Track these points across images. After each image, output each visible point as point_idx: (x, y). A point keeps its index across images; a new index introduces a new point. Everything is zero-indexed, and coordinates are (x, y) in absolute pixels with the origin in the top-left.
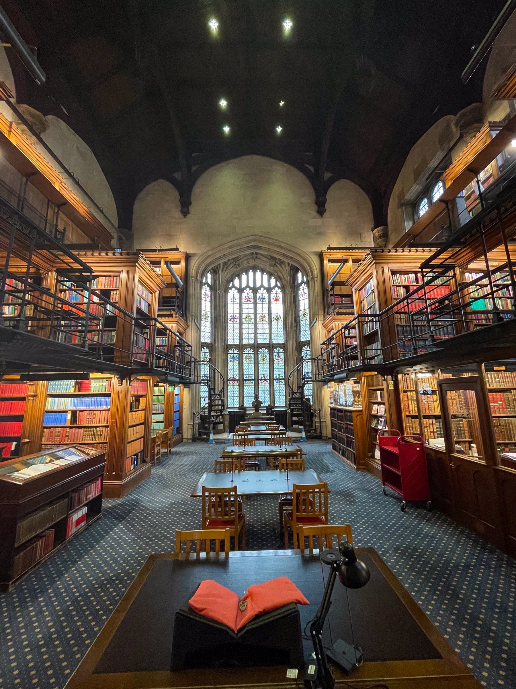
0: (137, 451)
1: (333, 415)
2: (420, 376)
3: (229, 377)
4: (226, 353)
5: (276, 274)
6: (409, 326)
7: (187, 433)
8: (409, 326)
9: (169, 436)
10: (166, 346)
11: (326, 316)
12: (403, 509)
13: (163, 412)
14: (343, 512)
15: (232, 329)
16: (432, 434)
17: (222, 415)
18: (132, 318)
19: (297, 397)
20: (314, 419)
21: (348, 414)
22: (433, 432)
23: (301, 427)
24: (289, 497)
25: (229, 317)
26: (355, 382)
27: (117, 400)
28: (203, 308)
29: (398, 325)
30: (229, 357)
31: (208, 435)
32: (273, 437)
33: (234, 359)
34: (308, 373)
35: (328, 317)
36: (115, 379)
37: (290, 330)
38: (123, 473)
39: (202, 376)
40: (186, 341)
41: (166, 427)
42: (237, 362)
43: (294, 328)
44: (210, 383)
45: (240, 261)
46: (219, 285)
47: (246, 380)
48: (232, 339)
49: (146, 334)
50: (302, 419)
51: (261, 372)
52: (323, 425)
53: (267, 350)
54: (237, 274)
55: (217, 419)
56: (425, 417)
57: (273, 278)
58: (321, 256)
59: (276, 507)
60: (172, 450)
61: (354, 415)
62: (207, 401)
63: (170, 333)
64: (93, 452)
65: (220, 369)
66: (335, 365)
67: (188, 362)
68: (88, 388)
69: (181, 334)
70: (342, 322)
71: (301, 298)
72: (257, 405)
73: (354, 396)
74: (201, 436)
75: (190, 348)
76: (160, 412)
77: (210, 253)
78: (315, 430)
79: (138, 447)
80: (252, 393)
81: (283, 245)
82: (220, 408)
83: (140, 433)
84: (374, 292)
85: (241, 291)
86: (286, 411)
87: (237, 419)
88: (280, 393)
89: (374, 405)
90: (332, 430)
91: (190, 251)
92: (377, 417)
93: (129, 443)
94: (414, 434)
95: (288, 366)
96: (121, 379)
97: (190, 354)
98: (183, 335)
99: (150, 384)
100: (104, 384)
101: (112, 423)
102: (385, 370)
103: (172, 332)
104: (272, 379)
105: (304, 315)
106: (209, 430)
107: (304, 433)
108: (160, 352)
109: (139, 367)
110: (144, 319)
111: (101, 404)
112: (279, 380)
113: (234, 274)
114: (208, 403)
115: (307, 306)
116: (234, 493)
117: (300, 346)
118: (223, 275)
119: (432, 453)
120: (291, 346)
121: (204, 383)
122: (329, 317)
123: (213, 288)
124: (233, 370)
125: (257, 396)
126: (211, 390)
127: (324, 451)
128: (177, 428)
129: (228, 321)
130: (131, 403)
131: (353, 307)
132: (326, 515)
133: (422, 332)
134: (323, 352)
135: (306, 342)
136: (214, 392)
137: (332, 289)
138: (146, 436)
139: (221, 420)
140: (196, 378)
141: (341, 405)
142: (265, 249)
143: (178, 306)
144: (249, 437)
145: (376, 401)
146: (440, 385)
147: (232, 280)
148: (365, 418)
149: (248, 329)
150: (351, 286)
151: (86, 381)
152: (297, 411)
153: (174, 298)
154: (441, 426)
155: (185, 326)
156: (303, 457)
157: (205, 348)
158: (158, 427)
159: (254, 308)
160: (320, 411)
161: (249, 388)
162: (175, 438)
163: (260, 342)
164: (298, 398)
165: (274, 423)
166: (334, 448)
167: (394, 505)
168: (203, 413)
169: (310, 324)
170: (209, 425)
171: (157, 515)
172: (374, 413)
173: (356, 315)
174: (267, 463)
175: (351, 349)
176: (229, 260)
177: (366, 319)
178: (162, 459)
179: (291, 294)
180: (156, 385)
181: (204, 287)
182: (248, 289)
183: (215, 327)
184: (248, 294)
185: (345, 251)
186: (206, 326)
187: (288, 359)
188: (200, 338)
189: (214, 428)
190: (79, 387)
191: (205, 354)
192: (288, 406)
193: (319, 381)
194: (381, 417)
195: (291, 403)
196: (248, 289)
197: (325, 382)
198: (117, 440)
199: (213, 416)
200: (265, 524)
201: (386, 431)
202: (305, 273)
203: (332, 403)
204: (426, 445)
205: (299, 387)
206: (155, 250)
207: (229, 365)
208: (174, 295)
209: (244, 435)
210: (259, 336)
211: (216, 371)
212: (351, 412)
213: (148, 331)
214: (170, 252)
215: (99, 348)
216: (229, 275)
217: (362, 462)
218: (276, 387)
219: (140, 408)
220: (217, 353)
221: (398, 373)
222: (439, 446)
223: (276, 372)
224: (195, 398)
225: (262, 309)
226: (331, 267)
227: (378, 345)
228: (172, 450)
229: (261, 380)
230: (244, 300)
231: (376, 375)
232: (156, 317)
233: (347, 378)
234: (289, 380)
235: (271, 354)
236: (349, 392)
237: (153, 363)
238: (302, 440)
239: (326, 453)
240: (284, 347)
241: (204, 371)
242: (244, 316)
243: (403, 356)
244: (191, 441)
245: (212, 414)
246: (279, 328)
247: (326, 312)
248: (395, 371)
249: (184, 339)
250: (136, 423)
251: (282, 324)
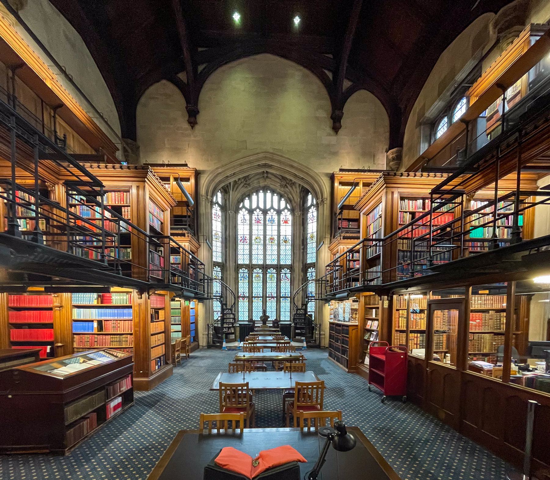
0: (160, 355)
1: (331, 328)
2: (412, 297)
4: (237, 272)
6: (410, 251)
7: (203, 341)
8: (410, 251)
9: (187, 343)
10: (179, 264)
11: (332, 240)
12: (383, 401)
13: (180, 323)
14: (334, 403)
15: (243, 250)
16: (415, 346)
17: (233, 327)
18: (146, 235)
20: (314, 331)
21: (345, 328)
22: (417, 344)
23: (303, 338)
24: (291, 392)
25: (239, 238)
26: (354, 301)
27: (138, 311)
28: (214, 228)
29: (399, 250)
30: (239, 276)
31: (221, 343)
32: (278, 345)
33: (244, 278)
34: (311, 293)
36: (135, 293)
37: (297, 252)
38: (150, 372)
41: (184, 336)
42: (247, 281)
48: (243, 259)
49: (160, 252)
50: (304, 331)
53: (275, 270)
56: (412, 332)
60: (190, 354)
61: (350, 329)
62: (220, 315)
64: (121, 355)
65: (232, 287)
66: (337, 286)
67: (201, 280)
68: (110, 300)
70: (348, 246)
71: (309, 221)
72: (265, 318)
75: (203, 266)
76: (177, 323)
78: (315, 341)
79: (160, 352)
80: (261, 309)
82: (231, 320)
83: (161, 340)
85: (251, 212)
86: (291, 324)
87: (247, 330)
88: (285, 309)
90: (330, 341)
92: (370, 331)
93: (152, 348)
94: (400, 345)
95: (293, 285)
96: (141, 292)
98: (196, 254)
99: (167, 298)
100: (125, 297)
101: (135, 331)
102: (382, 291)
105: (312, 237)
107: (305, 343)
109: (156, 283)
110: (157, 236)
111: (124, 315)
115: (315, 230)
116: (245, 388)
117: (306, 267)
119: (413, 360)
120: (298, 267)
122: (335, 241)
124: (243, 288)
125: (264, 312)
126: (224, 305)
127: (322, 357)
129: (239, 242)
130: (152, 315)
131: (359, 232)
132: (321, 405)
133: (420, 257)
134: (327, 273)
135: (311, 264)
136: (226, 307)
138: (167, 342)
139: (233, 331)
140: (209, 294)
141: (339, 321)
143: (189, 225)
144: (258, 345)
145: (371, 317)
146: (429, 305)
148: (359, 331)
149: (258, 250)
151: (107, 295)
153: (185, 217)
154: (424, 339)
155: (197, 245)
156: (304, 361)
158: (176, 336)
161: (257, 304)
162: (193, 345)
163: (268, 262)
165: (279, 335)
166: (330, 355)
167: (376, 398)
168: (216, 325)
169: (317, 247)
170: (222, 335)
171: (181, 404)
172: (368, 327)
173: (361, 239)
174: (273, 366)
175: (353, 272)
178: (181, 362)
179: (300, 216)
180: (173, 300)
182: (258, 210)
183: (226, 247)
186: (217, 246)
187: (294, 279)
188: (212, 258)
189: (226, 338)
190: (102, 299)
191: (217, 273)
192: (292, 320)
193: (321, 300)
194: (373, 331)
196: (258, 210)
197: (327, 301)
198: (141, 345)
199: (225, 327)
200: (270, 411)
201: (377, 343)
204: (409, 354)
205: (303, 305)
209: (254, 343)
210: (268, 257)
212: (347, 326)
213: (162, 249)
215: (117, 265)
217: (353, 367)
218: (282, 304)
219: (160, 319)
220: (228, 272)
221: (393, 294)
222: (420, 355)
223: (283, 290)
224: (209, 312)
227: (379, 268)
228: (190, 354)
229: (269, 297)
230: (253, 222)
232: (169, 235)
233: (347, 298)
234: (294, 298)
235: (279, 274)
236: (348, 310)
239: (324, 359)
241: (217, 288)
242: (254, 237)
243: (400, 279)
247: (333, 235)
248: (391, 292)
250: (157, 332)
251: (290, 247)
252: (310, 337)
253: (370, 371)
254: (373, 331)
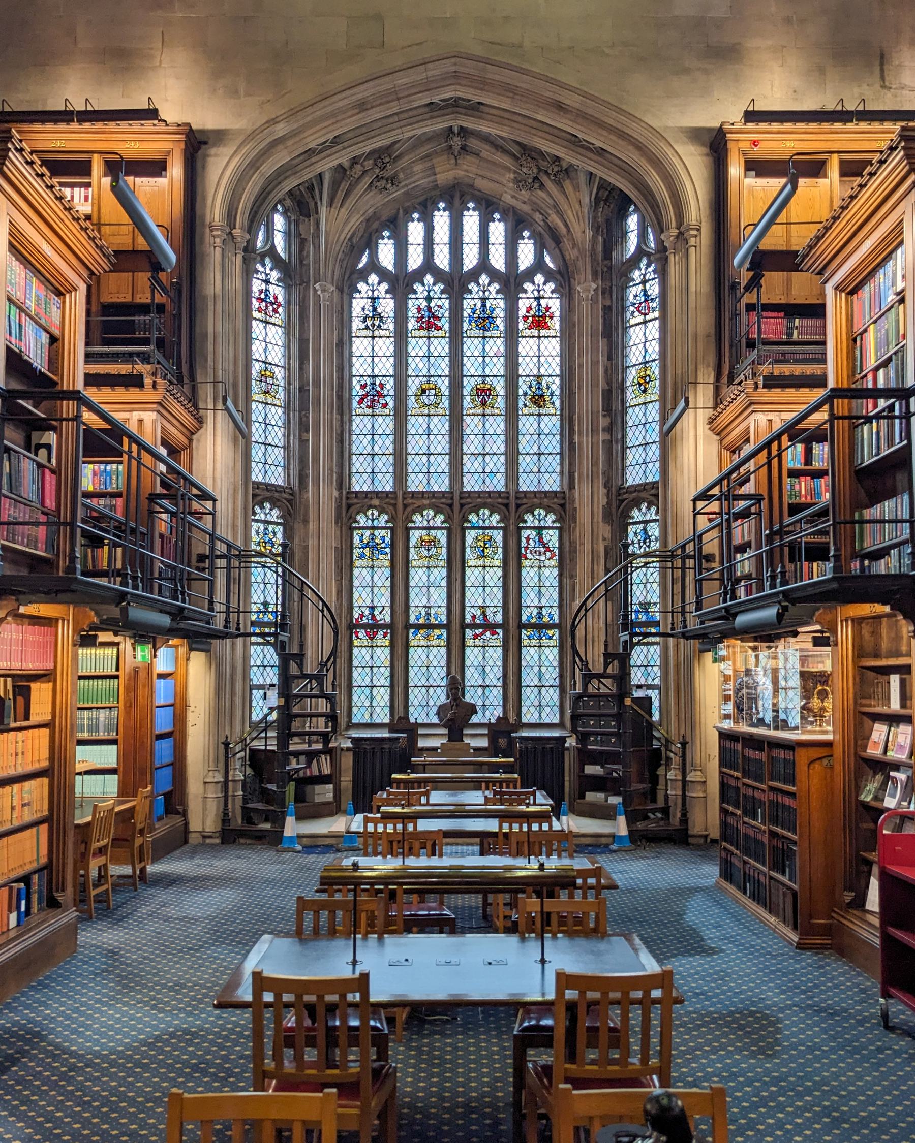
3: (356, 616)
5: (538, 217)
7: (203, 812)
10: (118, 495)
11: (725, 390)
19: (603, 690)
28: (257, 349)
30: (356, 540)
31: (279, 820)
35: (729, 392)
37: (584, 441)
39: (254, 608)
40: (194, 478)
42: (384, 561)
43: (602, 437)
44: (284, 636)
45: (403, 162)
46: (317, 261)
47: (418, 627)
48: (370, 473)
49: (43, 452)
51: (473, 598)
52: (695, 793)
54: (386, 215)
55: (309, 764)
57: (526, 234)
58: (716, 144)
59: (505, 1049)
60: (151, 869)
62: (274, 698)
63: (135, 447)
65: (324, 585)
67: (202, 558)
69: (174, 451)
72: (457, 715)
73: (804, 688)
74: (252, 822)
75: (209, 505)
77: (281, 129)
80: (439, 675)
81: (571, 100)
82: (321, 724)
84: (902, 301)
85: (401, 283)
87: (384, 763)
89: (877, 726)
90: (724, 811)
91: (205, 118)
92: (883, 767)
95: (572, 577)
97: (209, 527)
98: (184, 456)
103: (142, 446)
104: (512, 624)
105: (643, 383)
106: (283, 805)
108: (99, 519)
112: (540, 627)
113: (375, 216)
114: (279, 707)
117: (622, 502)
118: (334, 223)
121: (262, 635)
122: (736, 396)
123: (293, 273)
124: (371, 589)
125: (456, 687)
126: (290, 659)
128: (168, 796)
129: (355, 404)
135: (644, 487)
136: (301, 666)
137: (754, 283)
139: (327, 771)
140: (233, 617)
142: (504, 117)
143: (160, 344)
145: (884, 710)
147: (370, 243)
149: (428, 434)
150: (820, 273)
152: (602, 743)
153: (144, 309)
155: (187, 419)
157: (268, 506)
158: (97, 789)
159: (447, 363)
160: (684, 744)
161: (428, 658)
162: (161, 828)
164: (606, 696)
166: (727, 874)
168: (258, 745)
174: (485, 917)
176: (354, 161)
177: (869, 407)
179: (594, 300)
181: (259, 267)
183: (303, 427)
184: (429, 299)
185: (813, 126)
186: (269, 420)
187: (573, 551)
188: (247, 470)
189: (300, 798)
191: (266, 528)
193: (685, 636)
195: (578, 708)
199: (297, 754)
202: (654, 219)
203: (727, 717)
205: (608, 657)
206: (65, 116)
207: (356, 572)
208: (144, 298)
210: (469, 464)
211: (310, 594)
213: (51, 438)
214: (124, 125)
216: (356, 221)
220: (312, 526)
225: (483, 357)
226: (753, 193)
228: (151, 869)
229: (473, 626)
230: (412, 324)
231: (887, 616)
232: (80, 385)
234: (574, 627)
235: (512, 532)
237: (73, 559)
238: (614, 847)
239: (697, 889)
240: (563, 506)
241: (264, 589)
242: (413, 385)
244: (218, 841)
245: (292, 748)
246: (541, 431)
247: (725, 376)
249: (181, 468)
251: (555, 420)
252: (644, 795)
253: (887, 939)
254: (896, 766)
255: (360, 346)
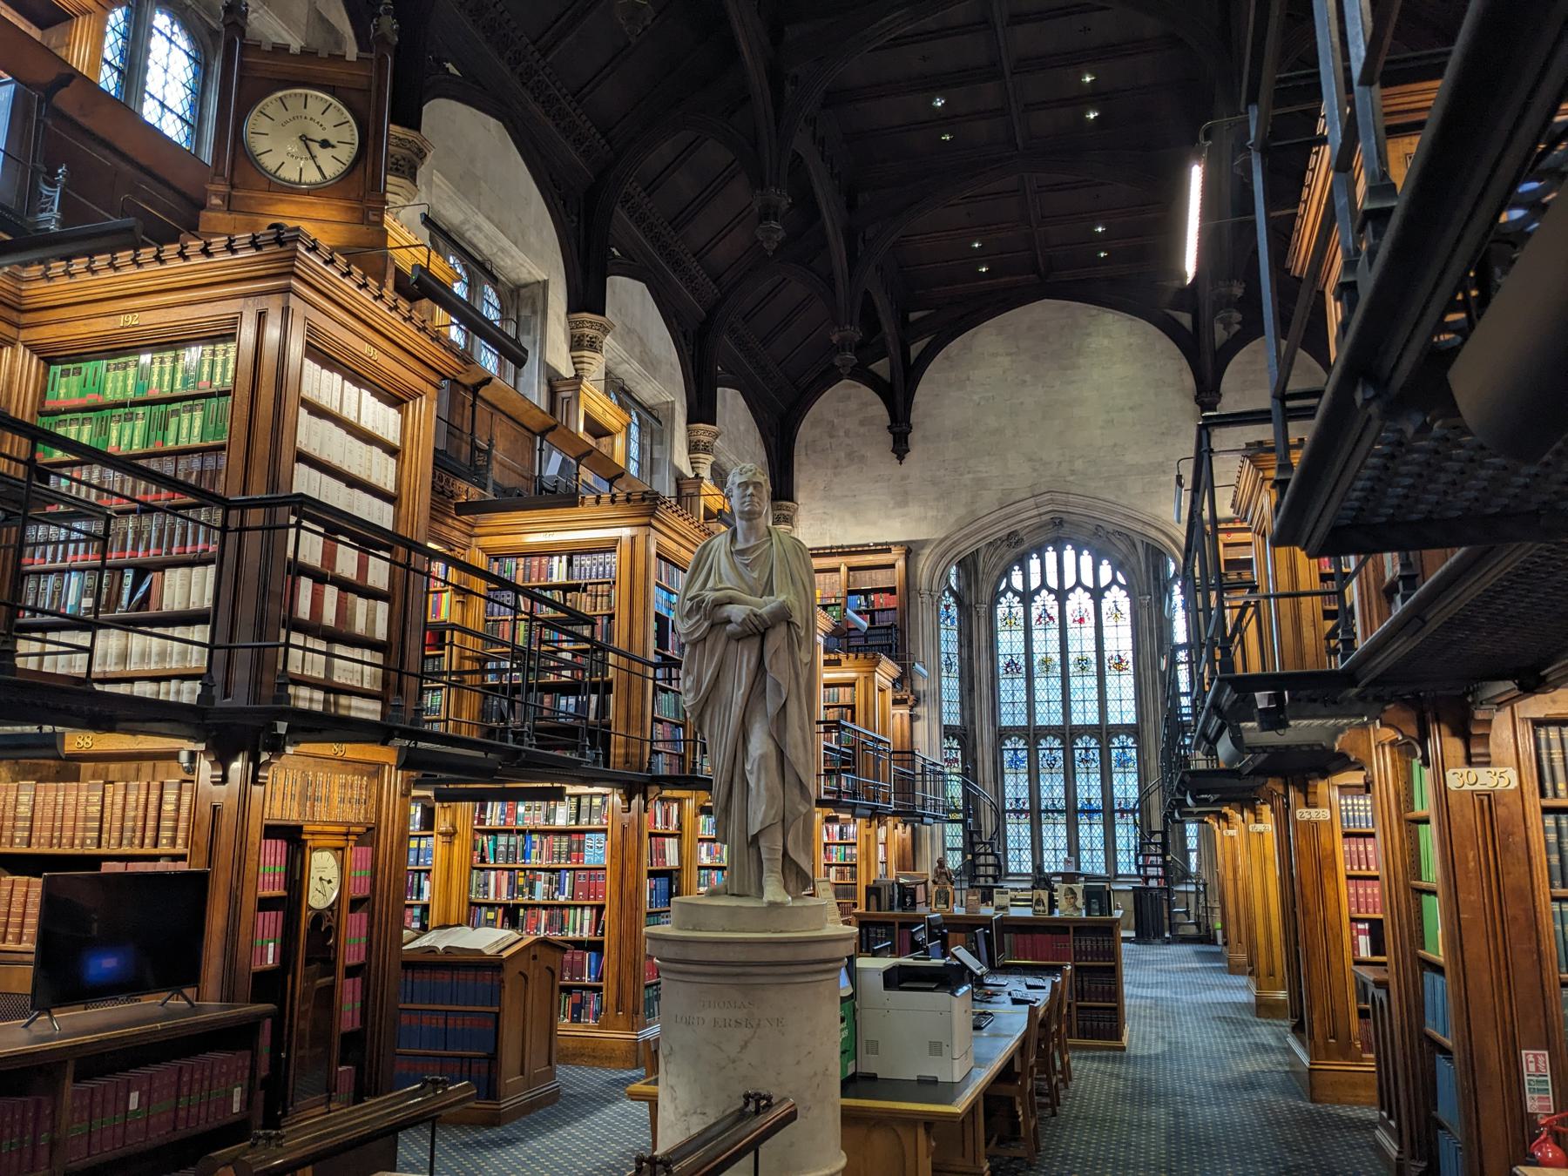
147: (1007, 573)
255: (1003, 637)
